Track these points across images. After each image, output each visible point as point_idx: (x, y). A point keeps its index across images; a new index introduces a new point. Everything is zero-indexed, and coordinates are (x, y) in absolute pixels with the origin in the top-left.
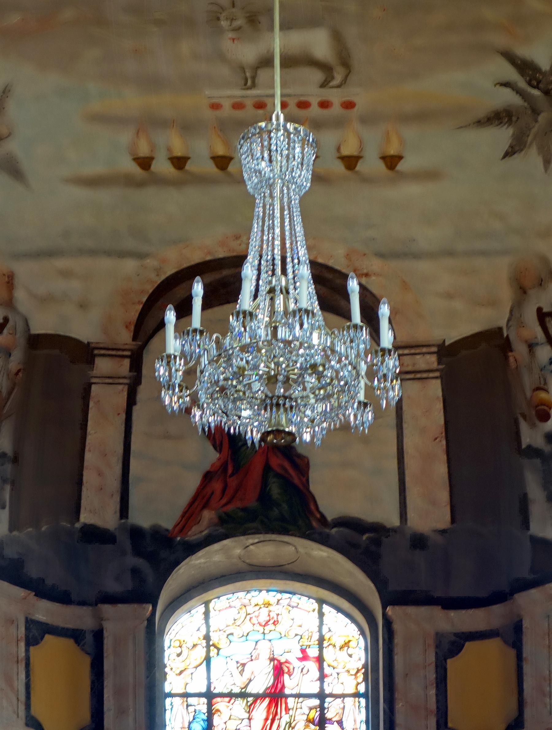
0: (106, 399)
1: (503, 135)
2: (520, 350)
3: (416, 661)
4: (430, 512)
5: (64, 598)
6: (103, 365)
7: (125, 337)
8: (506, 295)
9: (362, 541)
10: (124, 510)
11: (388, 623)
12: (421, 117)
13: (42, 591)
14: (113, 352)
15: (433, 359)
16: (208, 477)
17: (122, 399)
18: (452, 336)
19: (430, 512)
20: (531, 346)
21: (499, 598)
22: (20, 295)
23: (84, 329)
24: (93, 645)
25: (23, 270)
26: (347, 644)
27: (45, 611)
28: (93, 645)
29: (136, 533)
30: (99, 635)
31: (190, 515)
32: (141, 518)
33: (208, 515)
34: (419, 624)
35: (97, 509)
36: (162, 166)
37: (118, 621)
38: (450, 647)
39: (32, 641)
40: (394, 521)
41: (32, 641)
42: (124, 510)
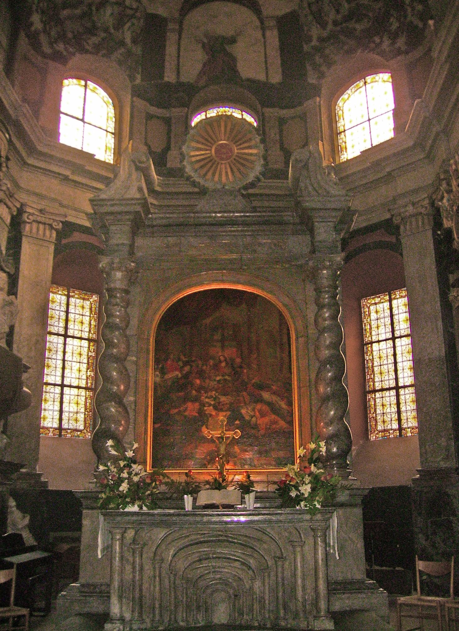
0: (172, 37)
5: (159, 105)
6: (171, 26)
7: (177, 15)
9: (255, 86)
11: (263, 114)
16: (204, 65)
18: (281, 13)
27: (153, 110)
28: (167, 121)
29: (181, 84)
30: (170, 118)
32: (183, 79)
33: (205, 78)
35: (169, 77)
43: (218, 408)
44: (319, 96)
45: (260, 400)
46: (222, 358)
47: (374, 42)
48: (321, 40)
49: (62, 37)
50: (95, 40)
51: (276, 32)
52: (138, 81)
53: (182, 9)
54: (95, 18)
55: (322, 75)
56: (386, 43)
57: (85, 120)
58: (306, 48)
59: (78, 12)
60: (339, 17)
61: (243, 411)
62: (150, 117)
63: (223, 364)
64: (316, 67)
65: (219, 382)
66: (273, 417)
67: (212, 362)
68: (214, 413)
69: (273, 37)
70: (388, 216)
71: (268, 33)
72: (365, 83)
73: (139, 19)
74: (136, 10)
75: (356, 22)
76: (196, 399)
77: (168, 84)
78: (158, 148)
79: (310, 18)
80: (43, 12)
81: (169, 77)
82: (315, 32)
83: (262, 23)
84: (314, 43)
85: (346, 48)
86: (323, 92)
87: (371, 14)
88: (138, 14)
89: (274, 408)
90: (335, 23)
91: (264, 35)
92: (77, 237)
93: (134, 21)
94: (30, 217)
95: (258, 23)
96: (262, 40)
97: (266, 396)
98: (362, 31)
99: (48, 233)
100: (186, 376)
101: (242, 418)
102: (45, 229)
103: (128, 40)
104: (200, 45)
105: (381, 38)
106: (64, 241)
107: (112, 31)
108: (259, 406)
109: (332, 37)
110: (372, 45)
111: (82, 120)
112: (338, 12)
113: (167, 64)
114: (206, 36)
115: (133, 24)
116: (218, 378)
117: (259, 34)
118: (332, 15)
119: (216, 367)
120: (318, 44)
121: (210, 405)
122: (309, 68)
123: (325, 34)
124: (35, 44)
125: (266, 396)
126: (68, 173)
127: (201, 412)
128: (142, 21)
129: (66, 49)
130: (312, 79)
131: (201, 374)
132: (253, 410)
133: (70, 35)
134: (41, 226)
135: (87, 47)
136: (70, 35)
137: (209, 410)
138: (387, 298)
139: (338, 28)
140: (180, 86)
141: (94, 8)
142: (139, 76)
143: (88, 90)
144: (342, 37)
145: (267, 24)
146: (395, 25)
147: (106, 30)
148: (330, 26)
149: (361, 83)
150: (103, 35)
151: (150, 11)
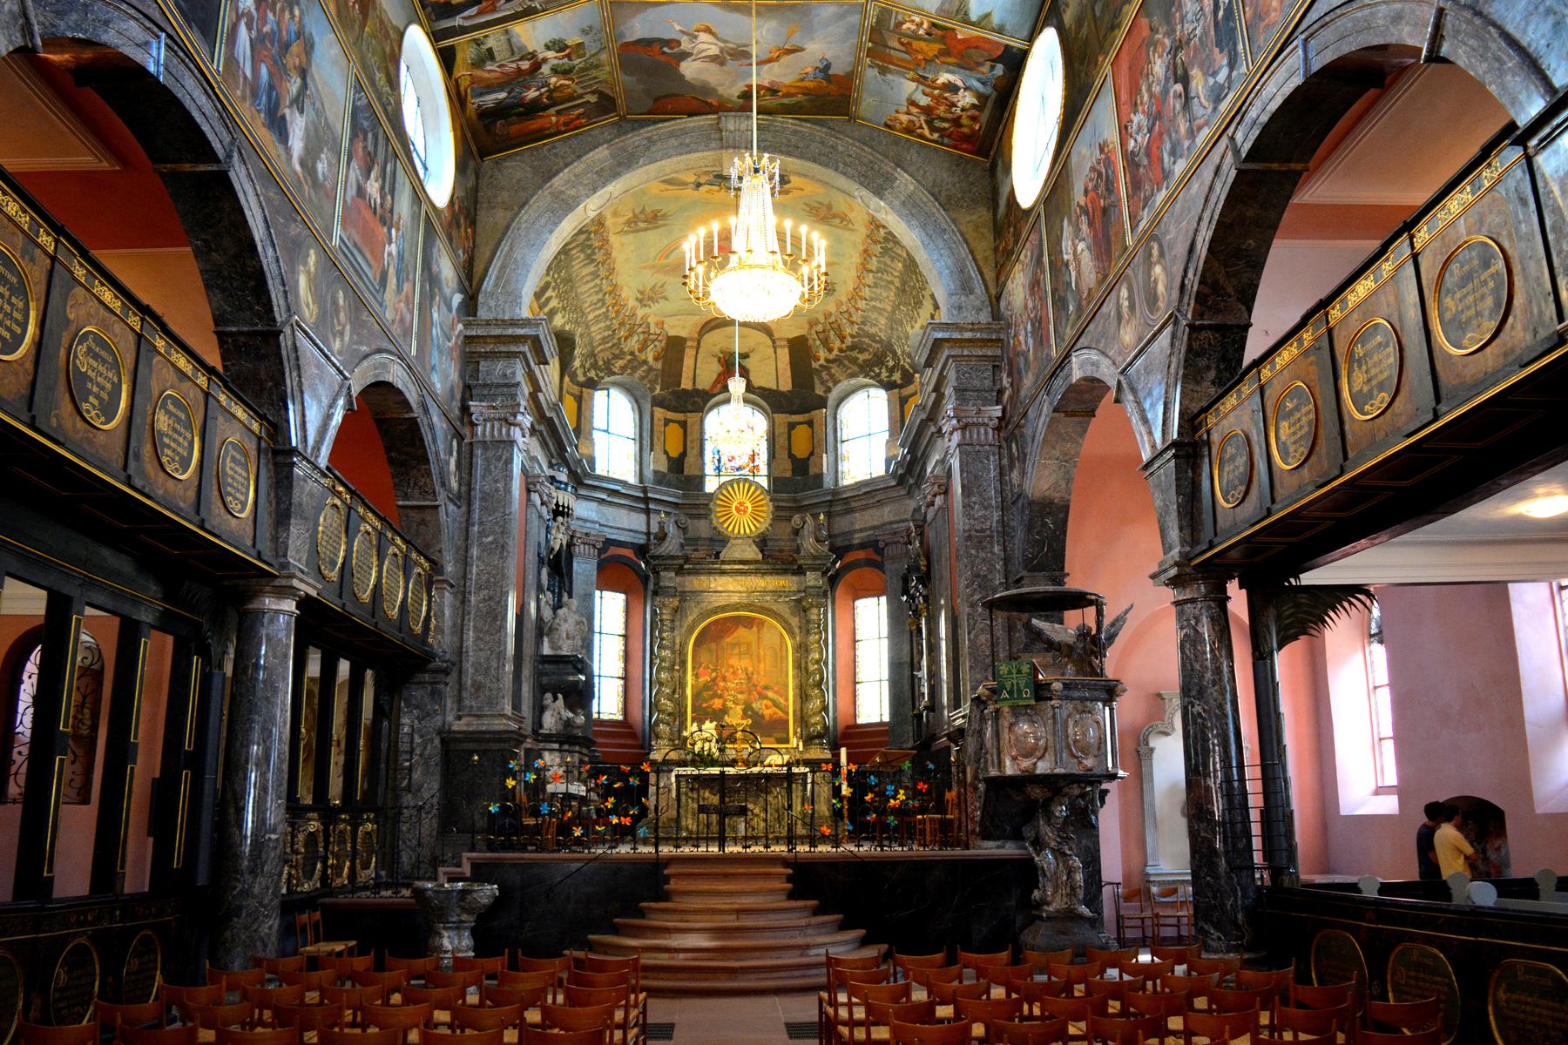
2: (811, 342)
3: (781, 430)
4: (786, 385)
5: (675, 410)
13: (668, 408)
14: (692, 339)
19: (786, 385)
21: (808, 411)
23: (683, 334)
24: (683, 425)
25: (667, 320)
26: (760, 423)
27: (671, 415)
28: (683, 425)
29: (696, 391)
31: (714, 386)
32: (700, 386)
34: (782, 419)
35: (686, 384)
37: (692, 418)
38: (792, 426)
39: (666, 425)
41: (666, 425)
45: (766, 697)
48: (827, 360)
49: (595, 366)
50: (621, 363)
55: (829, 390)
56: (884, 374)
58: (814, 365)
62: (667, 422)
64: (823, 382)
69: (784, 355)
81: (686, 384)
82: (822, 354)
83: (774, 342)
84: (822, 362)
86: (830, 403)
90: (841, 350)
92: (613, 551)
100: (714, 680)
103: (650, 359)
113: (684, 375)
118: (837, 344)
122: (816, 381)
123: (831, 357)
125: (770, 694)
130: (819, 391)
131: (724, 679)
137: (730, 704)
140: (696, 392)
146: (891, 363)
147: (632, 353)
148: (835, 352)
151: (672, 333)
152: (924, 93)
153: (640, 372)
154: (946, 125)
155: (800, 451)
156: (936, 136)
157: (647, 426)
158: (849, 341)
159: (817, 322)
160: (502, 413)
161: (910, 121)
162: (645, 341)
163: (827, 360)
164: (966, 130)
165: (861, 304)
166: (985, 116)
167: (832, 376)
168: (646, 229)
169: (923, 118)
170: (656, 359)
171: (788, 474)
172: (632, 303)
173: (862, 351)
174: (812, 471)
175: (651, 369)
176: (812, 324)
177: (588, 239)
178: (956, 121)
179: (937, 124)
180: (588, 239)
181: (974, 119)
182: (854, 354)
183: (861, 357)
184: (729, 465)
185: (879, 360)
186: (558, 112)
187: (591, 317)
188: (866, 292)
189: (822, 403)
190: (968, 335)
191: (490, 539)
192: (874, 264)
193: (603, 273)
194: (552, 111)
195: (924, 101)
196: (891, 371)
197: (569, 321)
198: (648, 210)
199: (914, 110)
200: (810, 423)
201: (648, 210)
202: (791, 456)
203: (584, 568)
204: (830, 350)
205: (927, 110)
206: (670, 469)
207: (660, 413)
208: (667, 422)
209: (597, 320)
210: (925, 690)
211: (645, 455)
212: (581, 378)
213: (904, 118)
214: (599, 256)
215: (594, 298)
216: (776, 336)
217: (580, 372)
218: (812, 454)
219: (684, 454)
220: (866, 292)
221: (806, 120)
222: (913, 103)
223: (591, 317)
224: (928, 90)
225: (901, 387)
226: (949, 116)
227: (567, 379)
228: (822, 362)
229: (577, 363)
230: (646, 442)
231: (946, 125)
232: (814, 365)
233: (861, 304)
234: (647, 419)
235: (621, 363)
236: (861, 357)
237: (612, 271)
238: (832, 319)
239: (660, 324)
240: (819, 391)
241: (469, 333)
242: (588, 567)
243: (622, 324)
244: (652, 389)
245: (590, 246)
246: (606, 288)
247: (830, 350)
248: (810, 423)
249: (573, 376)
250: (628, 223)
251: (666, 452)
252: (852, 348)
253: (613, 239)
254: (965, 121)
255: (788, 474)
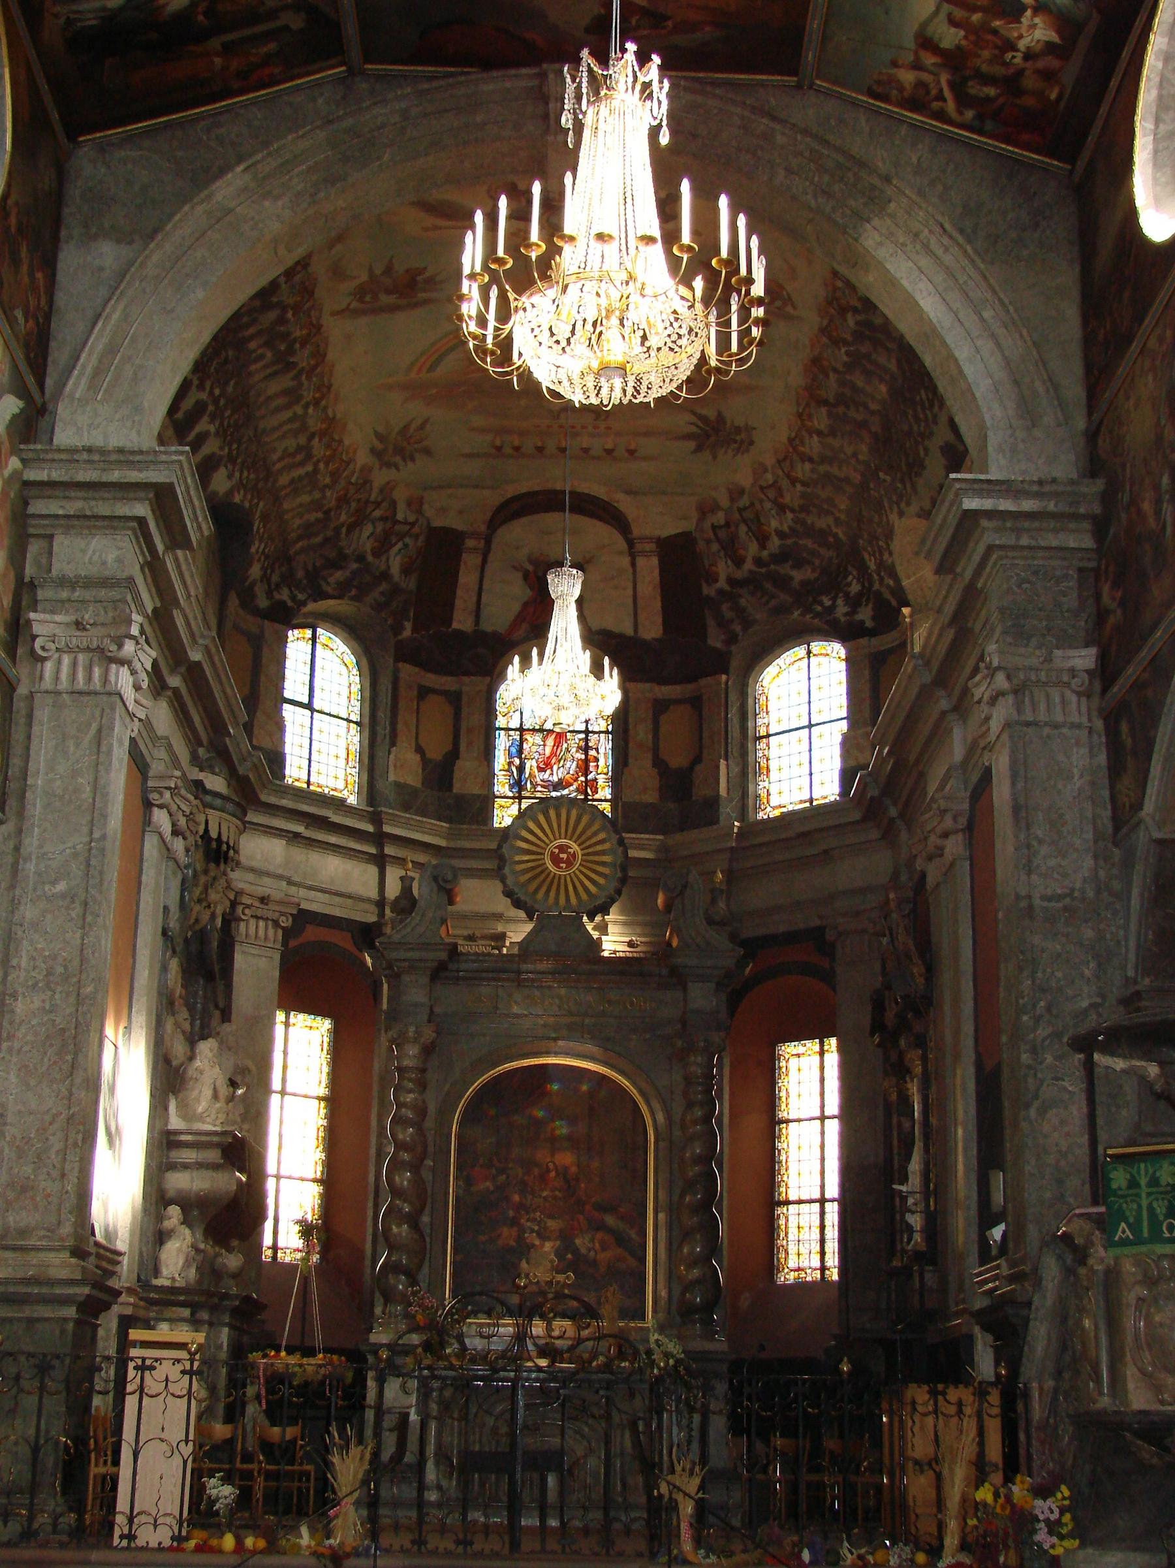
0: (470, 560)
1: (692, 445)
2: (701, 544)
6: (470, 543)
8: (695, 515)
10: (477, 622)
12: (648, 434)
13: (425, 666)
14: (474, 535)
15: (653, 546)
16: (526, 605)
17: (479, 561)
18: (665, 533)
19: (652, 630)
20: (708, 542)
21: (691, 678)
22: (426, 507)
24: (455, 699)
27: (431, 680)
32: (487, 627)
35: (462, 622)
36: (508, 450)
37: (470, 685)
40: (629, 631)
42: (477, 622)
43: (543, 1236)
44: (727, 673)
46: (551, 1165)
47: (821, 603)
48: (731, 581)
49: (288, 579)
50: (339, 575)
51: (655, 561)
52: (407, 633)
53: (491, 521)
54: (343, 543)
56: (842, 609)
57: (316, 706)
59: (318, 540)
60: (765, 553)
61: (577, 1241)
62: (424, 692)
63: (553, 1174)
64: (722, 624)
65: (545, 1198)
66: (619, 1251)
67: (536, 1171)
68: (537, 1242)
69: (649, 567)
70: (818, 922)
71: (641, 561)
72: (809, 652)
73: (417, 537)
74: (413, 524)
75: (793, 567)
76: (514, 1222)
77: (459, 634)
78: (436, 753)
79: (715, 547)
80: (267, 557)
81: (462, 622)
82: (723, 569)
83: (631, 544)
84: (722, 584)
85: (773, 603)
86: (734, 664)
87: (817, 562)
88: (416, 530)
89: (620, 1240)
90: (758, 561)
91: (633, 565)
92: (312, 933)
93: (407, 540)
94: (247, 911)
95: (622, 544)
96: (630, 570)
97: (610, 1220)
98: (804, 583)
99: (271, 932)
101: (576, 1252)
102: (266, 928)
104: (520, 574)
105: (834, 600)
106: (293, 943)
107: (370, 558)
108: (599, 1235)
109: (752, 582)
110: (819, 608)
111: (309, 706)
112: (763, 546)
113: (458, 603)
114: (530, 561)
115: (406, 546)
116: (545, 1194)
117: (626, 561)
118: (753, 549)
119: (543, 1178)
120: (727, 587)
121: (532, 1231)
122: (711, 623)
123: (739, 575)
124: (247, 599)
125: (610, 1220)
126: (300, 829)
127: (520, 1239)
128: (421, 538)
129: (293, 598)
130: (715, 640)
132: (592, 1240)
133: (300, 574)
134: (262, 923)
135: (329, 590)
136: (300, 574)
138: (817, 1048)
139: (763, 570)
141: (344, 530)
142: (408, 625)
143: (318, 646)
144: (768, 586)
145: (639, 547)
146: (855, 588)
147: (361, 558)
148: (749, 565)
149: (800, 651)
150: (355, 566)
151: (437, 523)
152: (952, 22)
153: (375, 595)
154: (991, 91)
155: (678, 761)
156: (970, 114)
157: (385, 698)
158: (775, 543)
159: (715, 507)
160: (94, 637)
161: (920, 84)
162: (387, 534)
163: (731, 581)
164: (1029, 101)
165: (803, 470)
166: (1071, 72)
167: (740, 612)
168: (393, 309)
169: (944, 78)
170: (406, 570)
171: (651, 797)
172: (363, 458)
173: (798, 565)
174: (700, 791)
175: (396, 590)
176: (705, 509)
177: (281, 320)
178: (1012, 83)
179: (975, 89)
180: (281, 320)
181: (1048, 76)
182: (785, 569)
183: (798, 576)
184: (540, 777)
185: (832, 582)
186: (228, 49)
187: (284, 480)
188: (813, 445)
189: (720, 663)
190: (1028, 505)
191: (61, 887)
192: (831, 387)
193: (308, 395)
194: (215, 43)
195: (950, 37)
196: (855, 603)
197: (240, 485)
198: (400, 268)
199: (930, 60)
200: (696, 703)
201: (400, 268)
202: (659, 763)
203: (255, 965)
204: (739, 562)
205: (954, 60)
206: (426, 782)
207: (408, 671)
208: (424, 692)
209: (296, 487)
210: (915, 1220)
211: (380, 753)
212: (263, 602)
213: (908, 77)
214: (302, 358)
215: (291, 443)
216: (636, 532)
217: (260, 591)
218: (698, 759)
219: (453, 755)
220: (813, 445)
221: (714, 83)
222: (926, 42)
223: (284, 480)
224: (959, 13)
225: (871, 633)
226: (999, 71)
227: (233, 601)
228: (722, 584)
229: (255, 571)
230: (383, 730)
231: (991, 91)
232: (707, 590)
233: (803, 470)
234: (385, 684)
235: (339, 575)
236: (798, 576)
237: (325, 389)
238: (744, 501)
239: (416, 504)
240: (715, 640)
241: (32, 475)
242: (263, 963)
243: (343, 500)
244: (397, 629)
245: (285, 336)
246: (314, 424)
247: (739, 562)
248: (696, 703)
249: (247, 599)
250: (360, 293)
251: (419, 750)
252: (781, 557)
253: (327, 321)
254: (1030, 82)
255: (651, 797)
